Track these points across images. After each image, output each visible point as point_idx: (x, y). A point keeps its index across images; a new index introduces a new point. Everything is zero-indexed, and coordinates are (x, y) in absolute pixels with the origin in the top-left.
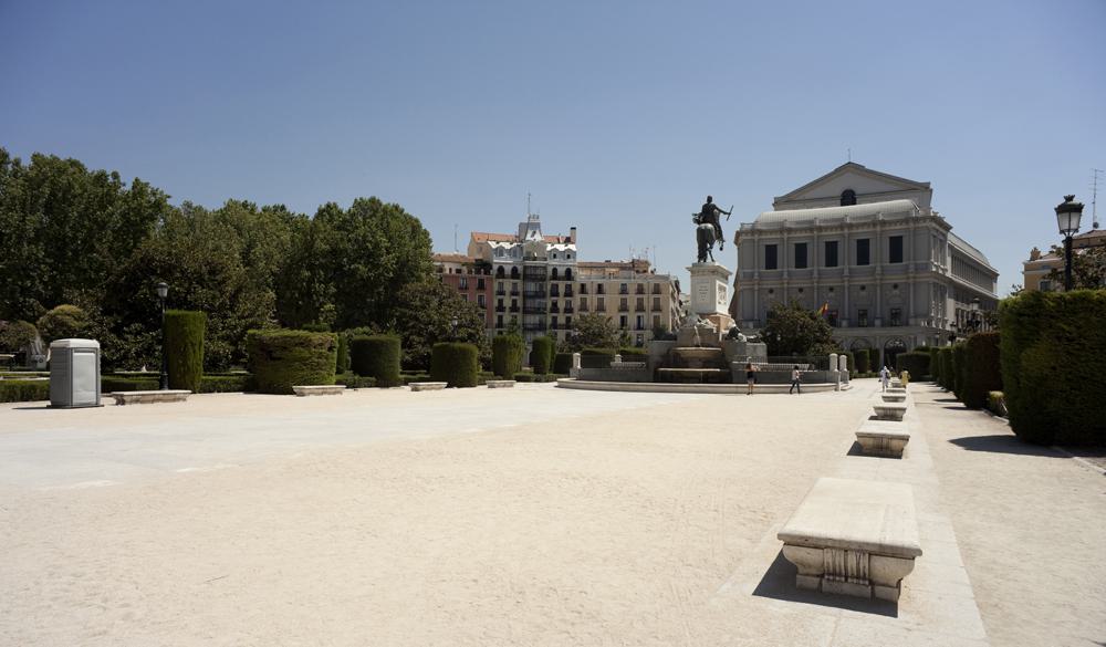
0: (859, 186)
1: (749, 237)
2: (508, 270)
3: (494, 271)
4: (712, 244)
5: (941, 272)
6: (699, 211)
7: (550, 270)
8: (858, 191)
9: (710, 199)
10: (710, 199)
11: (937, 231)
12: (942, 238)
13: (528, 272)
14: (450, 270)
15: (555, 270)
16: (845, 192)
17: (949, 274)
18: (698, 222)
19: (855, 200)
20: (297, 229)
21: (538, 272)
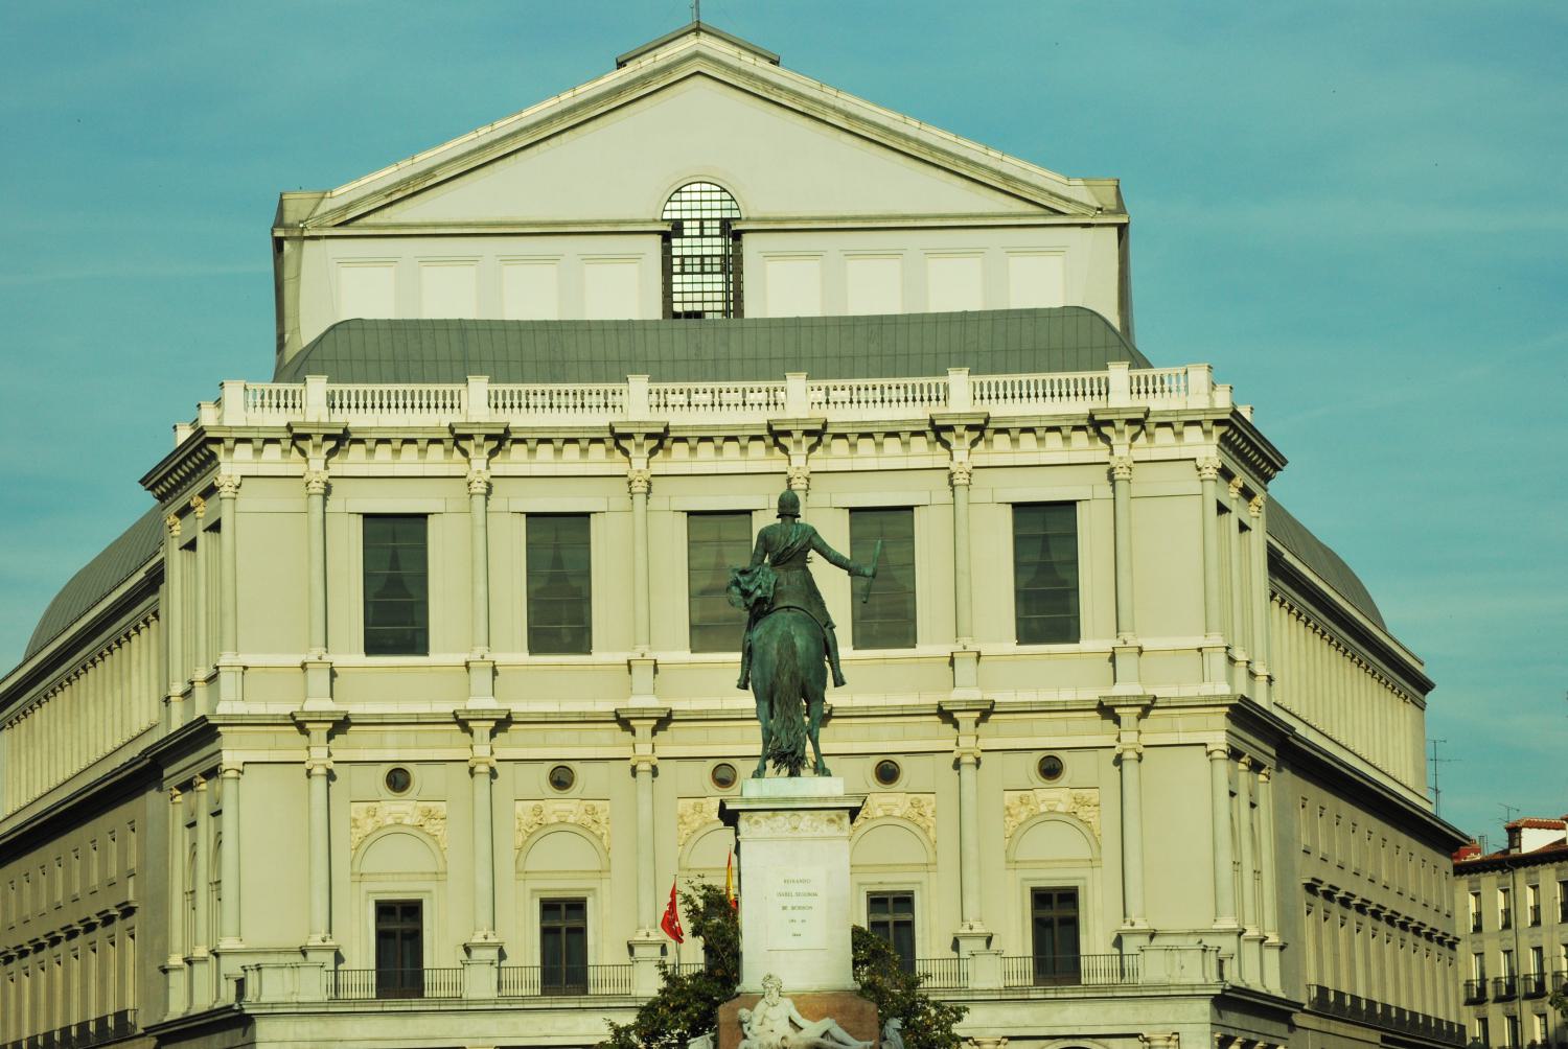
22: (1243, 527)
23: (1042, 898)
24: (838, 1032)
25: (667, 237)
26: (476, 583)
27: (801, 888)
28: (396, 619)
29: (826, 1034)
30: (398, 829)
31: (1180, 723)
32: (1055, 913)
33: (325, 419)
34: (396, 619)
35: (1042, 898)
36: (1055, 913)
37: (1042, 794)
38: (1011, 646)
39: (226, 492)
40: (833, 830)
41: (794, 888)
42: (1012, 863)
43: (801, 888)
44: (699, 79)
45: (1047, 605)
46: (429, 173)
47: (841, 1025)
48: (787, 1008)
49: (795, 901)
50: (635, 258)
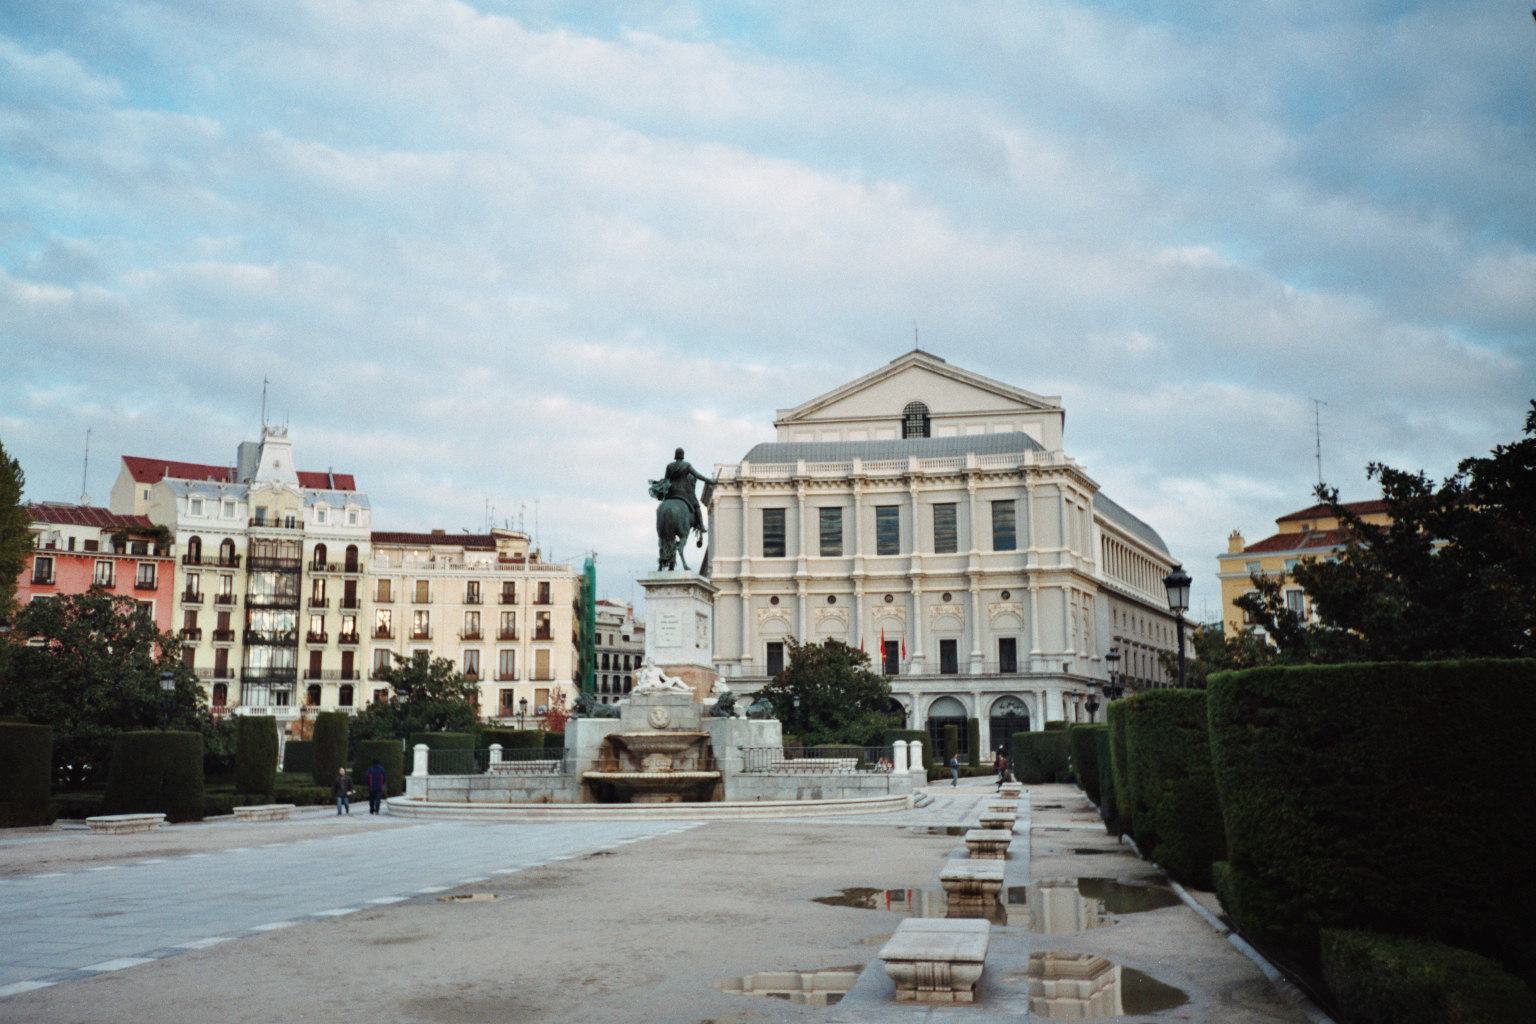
0: (938, 396)
1: (731, 491)
2: (211, 547)
3: (180, 547)
4: (684, 536)
5: (1082, 569)
6: (660, 475)
7: (309, 547)
8: (934, 408)
9: (679, 454)
10: (679, 454)
11: (1074, 491)
12: (1082, 505)
13: (260, 552)
14: (72, 540)
15: (321, 549)
16: (910, 407)
17: (1099, 574)
18: (659, 495)
19: (927, 420)
20: (258, 566)
21: (282, 553)
22: (1080, 508)
23: (1003, 642)
24: (680, 683)
25: (904, 421)
26: (804, 531)
27: (671, 619)
28: (775, 543)
29: (675, 684)
30: (774, 617)
31: (1052, 579)
32: (1008, 647)
33: (748, 476)
34: (775, 543)
35: (1003, 642)
36: (1008, 647)
37: (1002, 605)
38: (991, 552)
39: (716, 502)
40: (684, 594)
41: (667, 620)
42: (993, 629)
43: (671, 619)
44: (913, 369)
45: (1004, 539)
46: (822, 403)
47: (683, 680)
48: (660, 672)
49: (669, 625)
50: (894, 428)
